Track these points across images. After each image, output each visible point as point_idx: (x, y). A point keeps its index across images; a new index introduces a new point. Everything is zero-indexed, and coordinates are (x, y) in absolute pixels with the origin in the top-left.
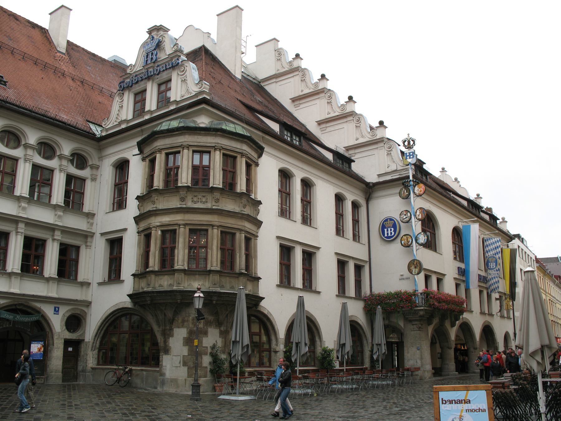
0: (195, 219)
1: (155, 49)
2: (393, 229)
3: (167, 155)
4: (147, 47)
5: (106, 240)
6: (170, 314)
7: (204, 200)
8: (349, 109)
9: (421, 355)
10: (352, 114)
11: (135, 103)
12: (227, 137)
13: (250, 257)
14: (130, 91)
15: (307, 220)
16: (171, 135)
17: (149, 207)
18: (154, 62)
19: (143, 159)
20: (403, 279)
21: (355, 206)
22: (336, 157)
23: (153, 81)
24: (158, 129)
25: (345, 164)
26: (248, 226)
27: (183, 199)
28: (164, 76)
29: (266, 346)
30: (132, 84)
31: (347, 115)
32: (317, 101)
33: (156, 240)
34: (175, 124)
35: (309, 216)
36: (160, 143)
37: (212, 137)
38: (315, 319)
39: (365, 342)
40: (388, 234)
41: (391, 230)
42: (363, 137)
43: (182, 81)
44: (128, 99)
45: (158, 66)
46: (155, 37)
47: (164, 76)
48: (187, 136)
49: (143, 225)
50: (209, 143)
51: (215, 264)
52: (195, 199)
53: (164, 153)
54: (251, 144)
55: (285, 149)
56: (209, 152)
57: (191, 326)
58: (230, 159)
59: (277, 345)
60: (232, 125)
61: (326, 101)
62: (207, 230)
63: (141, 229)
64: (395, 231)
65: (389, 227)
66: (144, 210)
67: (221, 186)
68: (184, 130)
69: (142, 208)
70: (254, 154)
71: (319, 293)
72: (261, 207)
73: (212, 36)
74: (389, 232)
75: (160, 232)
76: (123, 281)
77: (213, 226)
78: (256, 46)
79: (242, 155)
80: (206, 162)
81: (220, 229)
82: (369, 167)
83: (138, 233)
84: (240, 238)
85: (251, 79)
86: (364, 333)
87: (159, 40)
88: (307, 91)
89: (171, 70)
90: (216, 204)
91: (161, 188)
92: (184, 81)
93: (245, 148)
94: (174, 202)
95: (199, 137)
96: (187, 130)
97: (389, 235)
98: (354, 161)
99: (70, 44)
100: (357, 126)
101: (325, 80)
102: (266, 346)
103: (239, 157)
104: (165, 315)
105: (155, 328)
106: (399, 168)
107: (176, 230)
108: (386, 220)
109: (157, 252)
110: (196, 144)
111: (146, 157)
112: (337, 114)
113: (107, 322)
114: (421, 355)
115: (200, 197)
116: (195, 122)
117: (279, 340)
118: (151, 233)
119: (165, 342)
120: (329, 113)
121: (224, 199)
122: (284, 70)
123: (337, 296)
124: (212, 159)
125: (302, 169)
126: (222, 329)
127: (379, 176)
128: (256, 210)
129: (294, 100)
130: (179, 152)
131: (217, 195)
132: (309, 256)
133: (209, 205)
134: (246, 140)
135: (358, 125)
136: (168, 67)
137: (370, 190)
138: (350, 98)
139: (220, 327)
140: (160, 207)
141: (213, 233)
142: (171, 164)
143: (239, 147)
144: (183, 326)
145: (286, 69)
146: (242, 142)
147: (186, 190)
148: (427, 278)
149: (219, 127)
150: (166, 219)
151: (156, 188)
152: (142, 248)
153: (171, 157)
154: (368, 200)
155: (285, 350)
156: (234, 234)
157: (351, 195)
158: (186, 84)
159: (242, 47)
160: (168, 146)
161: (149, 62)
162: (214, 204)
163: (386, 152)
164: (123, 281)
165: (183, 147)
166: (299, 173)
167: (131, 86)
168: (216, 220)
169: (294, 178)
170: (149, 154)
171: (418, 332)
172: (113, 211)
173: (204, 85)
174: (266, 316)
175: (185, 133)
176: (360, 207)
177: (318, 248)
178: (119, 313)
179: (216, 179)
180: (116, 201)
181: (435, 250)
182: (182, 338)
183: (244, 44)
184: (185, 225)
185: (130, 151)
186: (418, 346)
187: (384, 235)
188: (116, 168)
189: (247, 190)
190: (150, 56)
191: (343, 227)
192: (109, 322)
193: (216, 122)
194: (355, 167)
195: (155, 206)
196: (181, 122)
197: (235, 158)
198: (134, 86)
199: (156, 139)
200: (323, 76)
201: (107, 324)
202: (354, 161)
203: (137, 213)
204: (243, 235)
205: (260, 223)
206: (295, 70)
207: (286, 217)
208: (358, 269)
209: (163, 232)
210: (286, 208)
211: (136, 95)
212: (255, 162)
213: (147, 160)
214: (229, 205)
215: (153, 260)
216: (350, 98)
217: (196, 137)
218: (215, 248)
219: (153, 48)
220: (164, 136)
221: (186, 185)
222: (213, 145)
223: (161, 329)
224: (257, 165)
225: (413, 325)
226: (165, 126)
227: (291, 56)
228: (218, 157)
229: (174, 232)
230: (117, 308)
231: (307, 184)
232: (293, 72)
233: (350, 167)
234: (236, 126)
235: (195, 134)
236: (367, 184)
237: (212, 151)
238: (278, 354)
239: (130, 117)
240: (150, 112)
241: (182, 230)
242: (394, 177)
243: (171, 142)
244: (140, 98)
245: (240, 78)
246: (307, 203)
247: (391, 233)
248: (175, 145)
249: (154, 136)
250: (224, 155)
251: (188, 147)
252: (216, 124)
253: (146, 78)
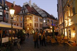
21: (42, 19)
36: (25, 16)
44: (22, 12)
70: (32, 16)
82: (43, 16)
99: (15, 5)
137: (43, 18)
157: (41, 18)
206: (36, 6)
227: (36, 5)
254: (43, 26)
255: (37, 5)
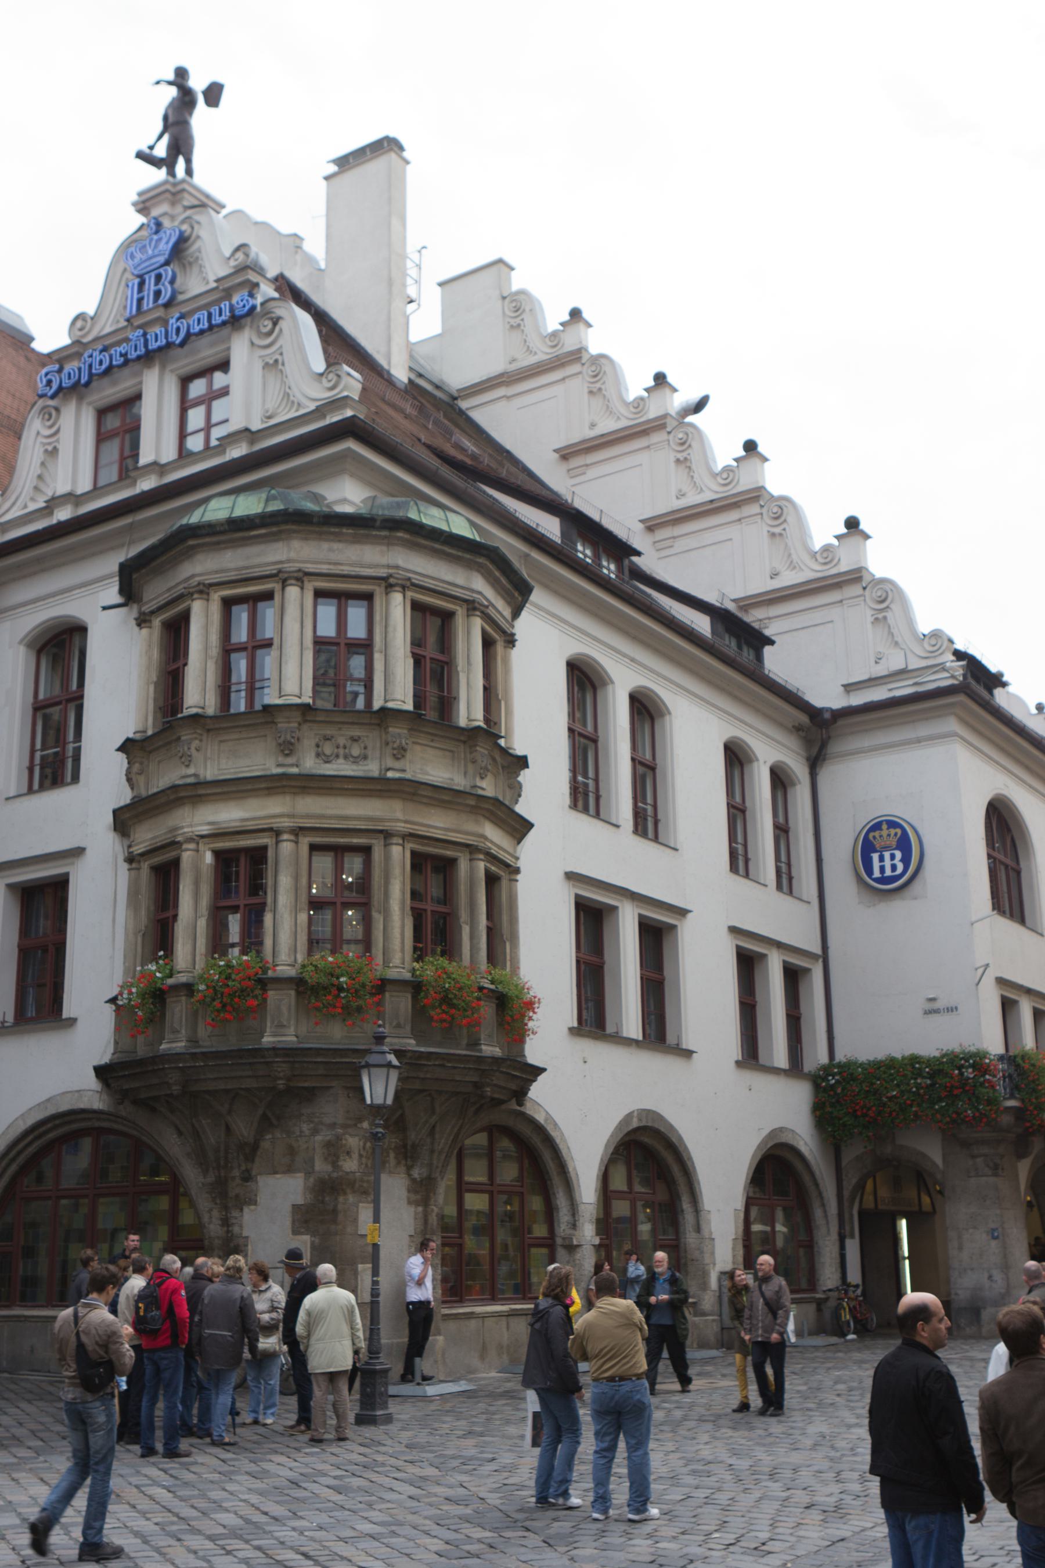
0: (329, 812)
1: (167, 263)
2: (898, 854)
3: (228, 603)
4: (139, 256)
5: (11, 887)
6: (244, 1127)
7: (356, 751)
8: (745, 483)
9: (1005, 1256)
10: (756, 495)
11: (101, 438)
12: (425, 547)
13: (500, 939)
14: (81, 399)
15: (648, 822)
16: (244, 539)
17: (168, 775)
18: (168, 305)
19: (142, 621)
20: (936, 1011)
21: (780, 779)
22: (720, 628)
23: (163, 368)
24: (195, 518)
25: (745, 648)
26: (494, 835)
27: (287, 748)
28: (205, 352)
29: (540, 1231)
30: (91, 375)
31: (742, 500)
32: (643, 458)
33: (197, 883)
34: (249, 505)
35: (649, 809)
36: (203, 566)
37: (378, 548)
38: (680, 1139)
39: (818, 1213)
40: (882, 869)
41: (893, 857)
42: (792, 566)
43: (266, 365)
44: (77, 426)
45: (182, 316)
46: (166, 223)
47: (205, 352)
48: (296, 544)
49: (146, 836)
50: (370, 566)
51: (396, 960)
52: (328, 749)
53: (216, 596)
54: (497, 574)
55: (585, 593)
56: (368, 597)
57: (321, 1166)
58: (434, 620)
59: (574, 1226)
60: (435, 512)
61: (672, 457)
62: (366, 851)
63: (138, 849)
64: (906, 860)
65: (887, 848)
66: (147, 784)
67: (409, 706)
68: (286, 522)
69: (142, 779)
71: (688, 1054)
72: (525, 777)
73: (307, 246)
74: (888, 863)
75: (209, 858)
76: (72, 1022)
77: (387, 835)
78: (440, 284)
79: (472, 606)
80: (356, 629)
81: (409, 846)
82: (815, 661)
83: (130, 859)
84: (471, 872)
85: (428, 387)
86: (817, 1185)
87: (181, 233)
88: (607, 425)
89: (226, 331)
90: (397, 765)
91: (210, 711)
92: (273, 366)
93: (479, 586)
94: (257, 759)
95: (336, 546)
96: (294, 522)
97: (888, 872)
98: (772, 642)
100: (773, 535)
101: (667, 391)
102: (540, 1231)
103: (460, 612)
104: (228, 1128)
105: (191, 1174)
106: (914, 664)
107: (265, 848)
108: (877, 827)
109: (202, 923)
110: (324, 568)
111: (152, 612)
112: (708, 496)
113: (13, 1160)
114: (1005, 1256)
115: (342, 741)
116: (317, 498)
117: (582, 1208)
118: (176, 863)
119: (226, 1222)
120: (681, 495)
121: (418, 748)
122: (532, 360)
123: (738, 1063)
124: (377, 617)
125: (633, 660)
126: (416, 1173)
127: (849, 688)
128: (511, 787)
129: (566, 454)
130: (268, 596)
131: (398, 731)
132: (656, 938)
133: (372, 768)
134: (481, 560)
135: (777, 530)
136: (217, 320)
137: (819, 731)
138: (750, 447)
139: (409, 1168)
140: (210, 773)
141: (387, 857)
142: (241, 634)
143: (460, 580)
144: (289, 1170)
145: (540, 357)
146: (470, 565)
147: (297, 716)
148: (1008, 1006)
149: (400, 514)
150: (230, 814)
151: (194, 711)
152: (143, 913)
153: (242, 616)
154: (815, 762)
155: (597, 1241)
156: (452, 862)
157: (770, 749)
158: (269, 386)
159: (409, 281)
160: (232, 576)
161: (148, 303)
162: (390, 762)
163: (869, 612)
164: (72, 1022)
165: (283, 578)
166: (625, 673)
167: (87, 384)
168: (399, 815)
169: (610, 687)
170: (162, 600)
171: (992, 1179)
172: (31, 791)
173: (345, 380)
174: (539, 1129)
175: (295, 531)
176: (793, 784)
177: (682, 912)
178: (56, 1127)
179: (397, 685)
180: (37, 761)
181: (1022, 921)
182: (290, 1209)
183: (412, 272)
184: (298, 832)
185: (89, 595)
186: (993, 1226)
187: (869, 871)
188: (39, 652)
189: (487, 720)
190: (151, 286)
191: (745, 845)
192: (21, 1159)
193: (384, 500)
194: (776, 662)
195: (191, 771)
196: (274, 498)
197: (447, 617)
198: (94, 384)
199: (189, 553)
200: (660, 379)
201: (14, 1168)
202: (772, 642)
203: (125, 796)
204: (481, 866)
205: (528, 826)
206: (567, 359)
207: (586, 810)
208: (793, 976)
209: (217, 854)
210: (586, 785)
211: (101, 414)
212: (504, 632)
213: (157, 622)
214: (433, 767)
215: (189, 947)
216: (750, 447)
217: (325, 545)
218: (395, 906)
219: (162, 259)
220: (218, 543)
221: (298, 701)
222: (382, 572)
223: (211, 1178)
224: (511, 641)
225: (973, 1157)
226: (218, 508)
227: (554, 318)
228: (397, 614)
229: (258, 857)
230: (51, 1111)
231: (645, 710)
232: (563, 365)
233: (759, 658)
234: (451, 516)
235: (320, 536)
236: (814, 713)
237: (378, 591)
238: (578, 1256)
239: (84, 485)
240: (157, 467)
241: (287, 847)
242: (898, 693)
243: (241, 563)
244: (119, 424)
245: (406, 381)
246: (647, 772)
247: (894, 868)
248: (257, 572)
249: (186, 541)
250: (417, 607)
251: (301, 577)
252: (386, 505)
253: (139, 358)
254: (817, 1055)
255: (595, 343)
